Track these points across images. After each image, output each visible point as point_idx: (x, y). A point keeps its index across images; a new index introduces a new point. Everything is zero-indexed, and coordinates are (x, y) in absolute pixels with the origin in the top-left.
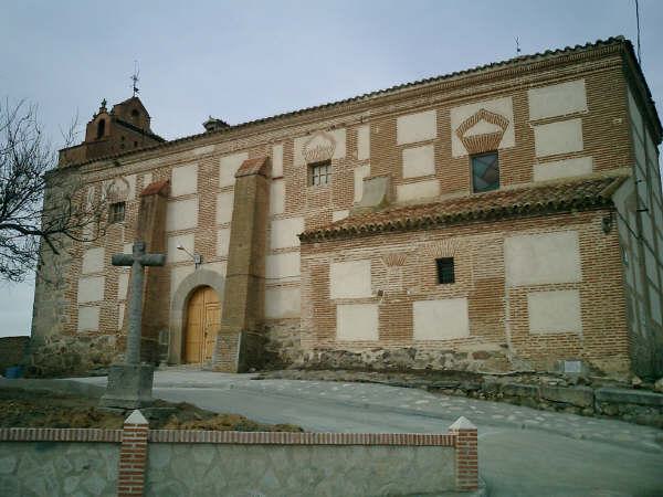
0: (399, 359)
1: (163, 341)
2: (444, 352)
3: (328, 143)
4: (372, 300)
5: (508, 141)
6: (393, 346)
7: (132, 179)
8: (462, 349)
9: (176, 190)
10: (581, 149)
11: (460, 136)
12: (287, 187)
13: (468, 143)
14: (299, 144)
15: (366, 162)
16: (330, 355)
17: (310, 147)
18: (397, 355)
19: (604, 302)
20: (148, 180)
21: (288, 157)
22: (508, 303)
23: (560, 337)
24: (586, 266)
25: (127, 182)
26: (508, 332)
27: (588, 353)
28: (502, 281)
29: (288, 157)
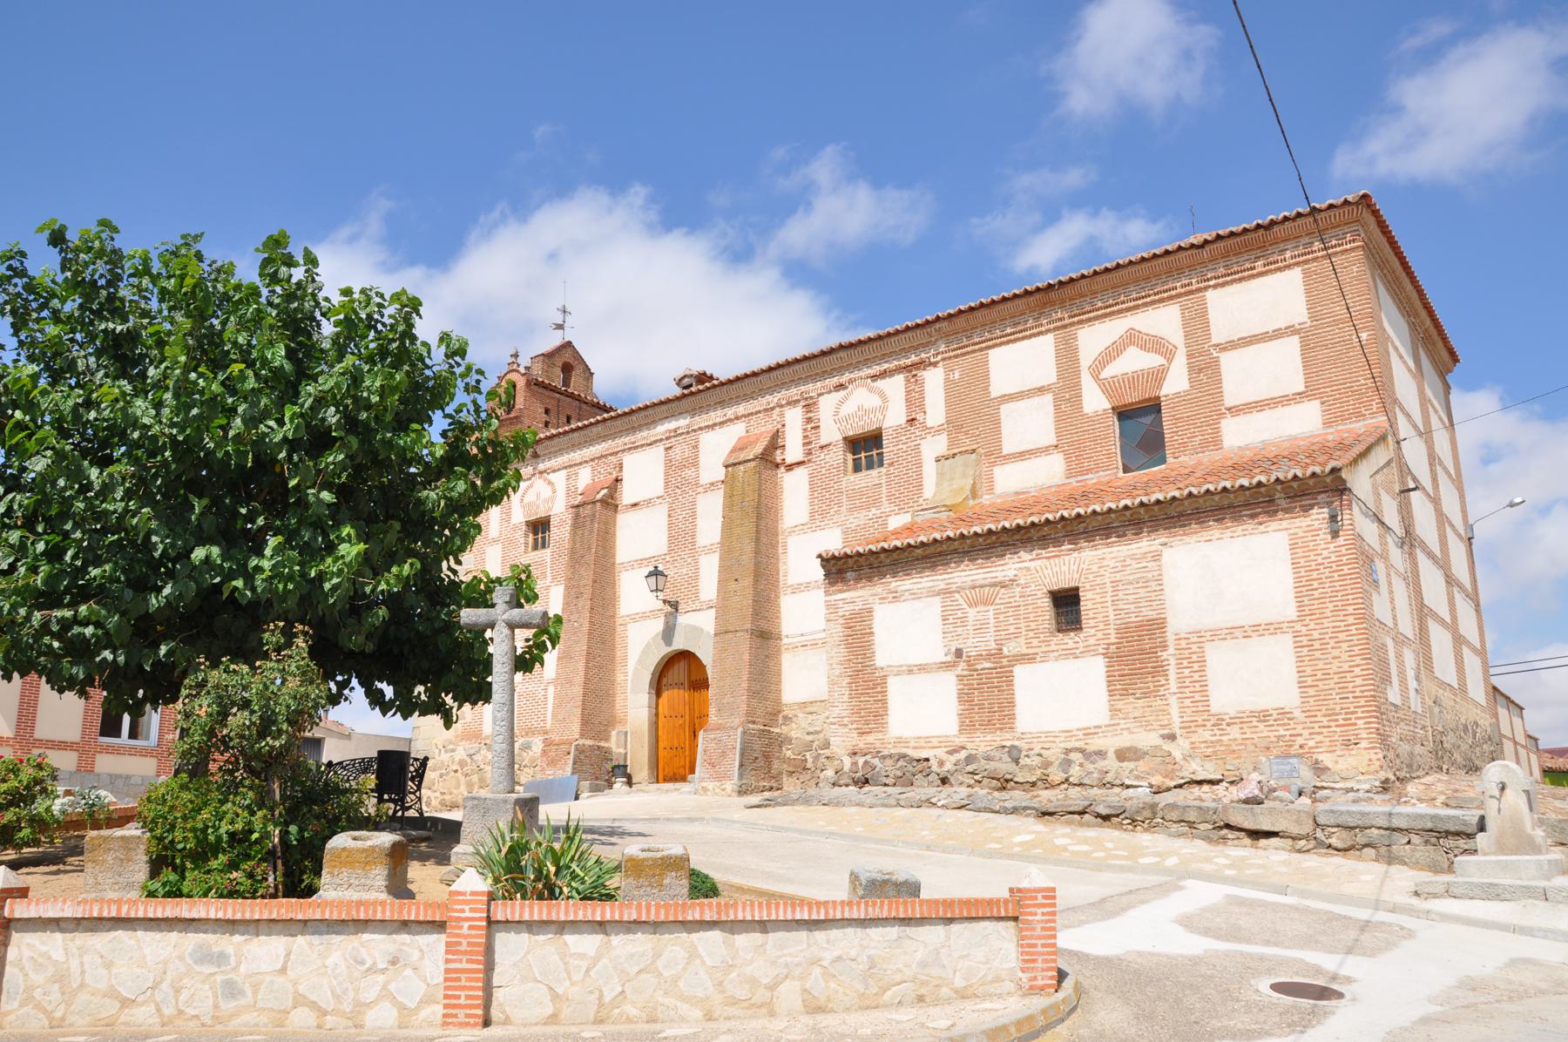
0: (992, 765)
1: (618, 747)
2: (1068, 751)
3: (873, 401)
4: (946, 666)
5: (1176, 383)
6: (982, 743)
7: (559, 478)
8: (1095, 744)
10: (1301, 388)
11: (1096, 378)
12: (811, 476)
13: (1107, 387)
14: (827, 404)
15: (938, 431)
16: (876, 761)
17: (849, 408)
18: (988, 759)
19: (1335, 653)
20: (585, 477)
21: (811, 424)
22: (1173, 662)
23: (1263, 716)
24: (1304, 590)
25: (550, 483)
26: (1175, 711)
27: (1311, 743)
28: (1156, 626)
29: (811, 424)
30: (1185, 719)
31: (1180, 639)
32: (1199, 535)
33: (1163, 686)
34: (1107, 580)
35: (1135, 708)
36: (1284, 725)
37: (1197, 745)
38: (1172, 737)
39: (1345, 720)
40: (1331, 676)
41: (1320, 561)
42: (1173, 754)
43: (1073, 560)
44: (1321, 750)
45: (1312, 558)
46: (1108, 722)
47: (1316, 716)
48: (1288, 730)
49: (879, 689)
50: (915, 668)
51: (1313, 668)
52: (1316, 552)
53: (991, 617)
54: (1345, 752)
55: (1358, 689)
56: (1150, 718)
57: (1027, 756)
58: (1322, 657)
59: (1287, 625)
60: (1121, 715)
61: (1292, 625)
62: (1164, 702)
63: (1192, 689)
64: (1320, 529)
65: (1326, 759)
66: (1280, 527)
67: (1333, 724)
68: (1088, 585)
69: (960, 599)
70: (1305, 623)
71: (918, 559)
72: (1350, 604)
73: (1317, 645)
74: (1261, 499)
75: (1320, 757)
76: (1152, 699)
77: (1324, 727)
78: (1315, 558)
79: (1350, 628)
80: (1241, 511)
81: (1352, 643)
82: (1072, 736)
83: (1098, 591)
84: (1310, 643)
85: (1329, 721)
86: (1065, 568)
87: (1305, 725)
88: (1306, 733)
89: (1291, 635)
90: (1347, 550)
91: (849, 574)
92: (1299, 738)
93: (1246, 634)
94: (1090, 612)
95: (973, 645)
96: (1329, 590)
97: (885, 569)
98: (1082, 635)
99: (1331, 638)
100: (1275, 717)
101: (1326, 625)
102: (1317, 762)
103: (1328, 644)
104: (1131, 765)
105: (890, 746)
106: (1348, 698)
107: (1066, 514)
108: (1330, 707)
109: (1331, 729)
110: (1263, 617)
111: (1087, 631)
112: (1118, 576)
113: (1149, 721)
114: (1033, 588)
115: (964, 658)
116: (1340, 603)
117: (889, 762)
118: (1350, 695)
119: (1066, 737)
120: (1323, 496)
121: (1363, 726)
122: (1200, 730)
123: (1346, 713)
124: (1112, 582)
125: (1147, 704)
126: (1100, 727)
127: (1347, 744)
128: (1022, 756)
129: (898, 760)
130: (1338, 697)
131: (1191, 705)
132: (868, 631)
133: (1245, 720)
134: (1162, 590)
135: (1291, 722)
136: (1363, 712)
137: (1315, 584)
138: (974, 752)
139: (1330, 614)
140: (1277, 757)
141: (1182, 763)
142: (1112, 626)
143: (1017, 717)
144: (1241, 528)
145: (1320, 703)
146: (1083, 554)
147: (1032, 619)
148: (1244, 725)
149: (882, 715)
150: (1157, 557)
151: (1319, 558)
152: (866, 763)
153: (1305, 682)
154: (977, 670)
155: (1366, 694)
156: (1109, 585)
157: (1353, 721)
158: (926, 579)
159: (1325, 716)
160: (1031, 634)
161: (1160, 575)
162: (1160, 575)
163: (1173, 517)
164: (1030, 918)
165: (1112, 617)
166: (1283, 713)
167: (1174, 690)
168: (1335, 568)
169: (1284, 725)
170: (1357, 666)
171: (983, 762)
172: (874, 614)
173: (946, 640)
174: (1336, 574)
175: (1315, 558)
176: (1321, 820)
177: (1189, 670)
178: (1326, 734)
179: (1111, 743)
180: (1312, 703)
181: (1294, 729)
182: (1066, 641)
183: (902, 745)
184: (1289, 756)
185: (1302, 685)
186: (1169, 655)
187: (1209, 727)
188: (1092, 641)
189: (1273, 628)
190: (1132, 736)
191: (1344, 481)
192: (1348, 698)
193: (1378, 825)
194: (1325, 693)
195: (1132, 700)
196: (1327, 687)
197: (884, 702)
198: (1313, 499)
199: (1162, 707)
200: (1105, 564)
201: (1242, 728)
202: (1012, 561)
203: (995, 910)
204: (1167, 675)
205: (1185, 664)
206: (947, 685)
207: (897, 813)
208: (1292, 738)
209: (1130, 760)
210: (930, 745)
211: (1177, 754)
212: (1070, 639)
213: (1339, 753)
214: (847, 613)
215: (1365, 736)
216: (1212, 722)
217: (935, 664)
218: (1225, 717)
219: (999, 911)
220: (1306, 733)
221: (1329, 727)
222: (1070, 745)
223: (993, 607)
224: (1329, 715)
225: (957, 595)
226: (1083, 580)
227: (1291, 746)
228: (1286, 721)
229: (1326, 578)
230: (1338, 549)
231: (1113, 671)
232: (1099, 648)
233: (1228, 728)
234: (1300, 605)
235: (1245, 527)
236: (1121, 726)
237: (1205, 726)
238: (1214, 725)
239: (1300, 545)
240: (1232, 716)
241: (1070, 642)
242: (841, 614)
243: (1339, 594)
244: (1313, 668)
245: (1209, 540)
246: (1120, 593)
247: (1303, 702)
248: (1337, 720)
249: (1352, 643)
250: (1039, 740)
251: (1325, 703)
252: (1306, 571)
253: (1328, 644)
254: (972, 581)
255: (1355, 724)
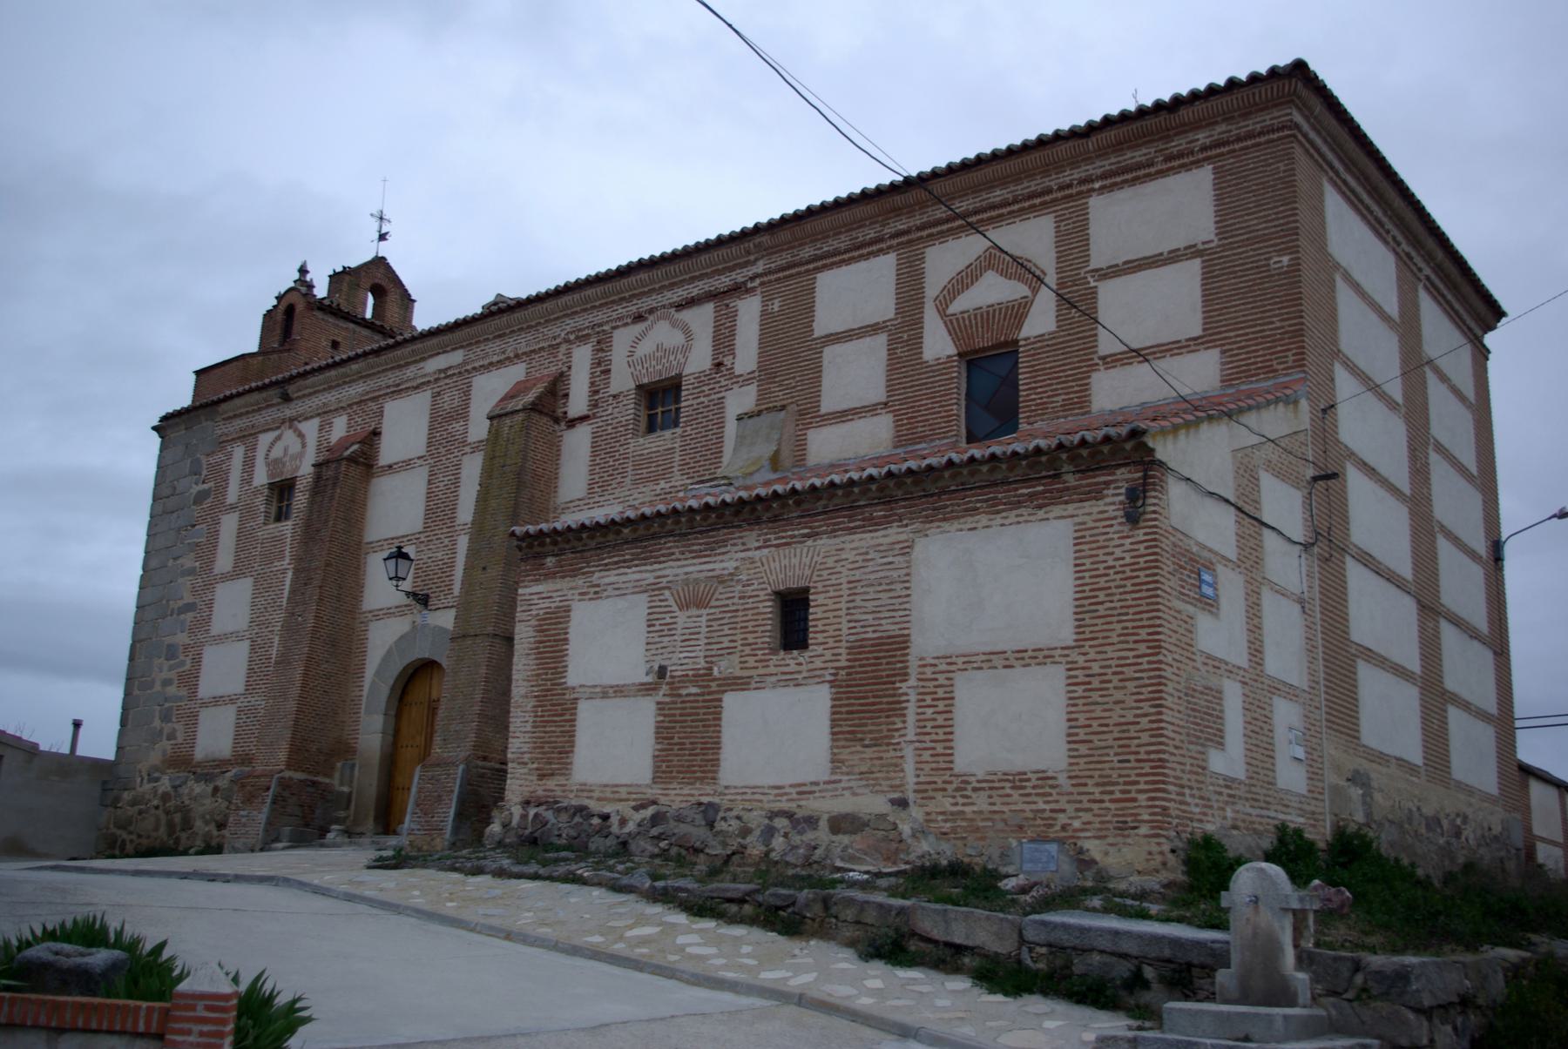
0: (682, 829)
1: (342, 784)
2: (773, 815)
3: (677, 338)
4: (646, 689)
5: (1041, 320)
6: (678, 797)
7: (310, 428)
8: (813, 805)
9: (388, 451)
10: (1197, 331)
11: (942, 313)
12: (595, 436)
13: (956, 326)
14: (622, 339)
15: (747, 380)
16: (549, 815)
17: (646, 347)
18: (679, 819)
19: (1118, 695)
20: (340, 428)
22: (913, 697)
23: (1018, 780)
24: (1086, 604)
25: (301, 435)
26: (909, 767)
27: (1077, 824)
28: (899, 644)
29: (601, 368)
30: (922, 779)
31: (925, 666)
32: (962, 520)
33: (897, 730)
34: (844, 580)
35: (862, 759)
36: (1044, 795)
37: (933, 816)
38: (902, 803)
39: (1123, 792)
40: (1111, 728)
41: (1111, 563)
42: (900, 826)
43: (805, 550)
44: (1088, 834)
45: (1102, 558)
46: (826, 778)
47: (1086, 785)
48: (1048, 802)
49: (567, 717)
50: (611, 691)
51: (1088, 715)
52: (1107, 550)
53: (704, 624)
54: (1120, 839)
55: (1142, 750)
56: (878, 775)
57: (724, 819)
58: (1100, 700)
59: (1059, 652)
60: (844, 769)
61: (1066, 652)
62: (899, 754)
63: (934, 737)
64: (1115, 518)
65: (1094, 848)
66: (1065, 514)
67: (1106, 797)
68: (819, 585)
69: (671, 599)
70: (1083, 650)
71: (627, 543)
72: (1143, 627)
73: (1096, 683)
74: (1044, 473)
75: (1087, 845)
76: (884, 748)
77: (1095, 801)
78: (1105, 558)
79: (1140, 660)
80: (1017, 489)
81: (1141, 682)
82: (781, 795)
83: (832, 594)
84: (1087, 679)
85: (1102, 793)
86: (795, 561)
87: (1072, 798)
88: (1070, 808)
89: (1062, 668)
90: (1146, 548)
91: (549, 559)
92: (1061, 816)
93: (1007, 663)
94: (819, 623)
95: (682, 661)
96: (1118, 605)
97: (588, 554)
98: (807, 654)
99: (1115, 673)
100: (1034, 782)
101: (1110, 655)
102: (1081, 851)
103: (1110, 681)
104: (845, 839)
105: (572, 796)
106: (1128, 761)
107: (798, 486)
108: (1104, 773)
109: (1104, 805)
110: (1029, 640)
111: (815, 649)
112: (858, 575)
113: (876, 779)
114: (755, 587)
115: (668, 679)
116: (1129, 624)
117: (564, 817)
118: (1132, 757)
119: (776, 795)
120: (1123, 470)
121: (1144, 803)
122: (939, 795)
123: (1126, 783)
124: (849, 582)
125: (876, 755)
126: (816, 784)
127: (1123, 828)
128: (719, 818)
129: (574, 814)
130: (1116, 759)
131: (930, 759)
132: (562, 637)
133: (996, 785)
134: (908, 595)
135: (1054, 792)
136: (1146, 783)
137: (1102, 596)
138: (664, 809)
139: (1115, 640)
140: (1032, 840)
141: (909, 841)
142: (844, 644)
143: (722, 764)
144: (1015, 512)
145: (1092, 766)
146: (819, 542)
147: (750, 629)
148: (994, 793)
149: (567, 752)
150: (906, 549)
151: (1109, 558)
152: (536, 815)
153: (1077, 734)
154: (680, 695)
155: (1152, 756)
156: (845, 586)
157: (1133, 795)
158: (634, 569)
159: (1097, 785)
160: (747, 650)
161: (908, 575)
162: (908, 575)
163: (932, 495)
164: (179, 1038)
165: (845, 631)
166: (1044, 778)
167: (911, 736)
168: (1129, 574)
169: (1044, 795)
170: (1146, 715)
171: (672, 823)
172: (572, 614)
173: (648, 654)
174: (1128, 583)
175: (1105, 558)
176: (1030, 935)
177: (932, 710)
178: (1096, 812)
179: (825, 806)
180: (1082, 766)
181: (1057, 801)
182: (788, 662)
183: (585, 794)
184: (1046, 840)
185: (1072, 740)
186: (909, 688)
187: (950, 792)
188: (818, 663)
189: (1037, 657)
190: (855, 798)
191: (1151, 451)
192: (1128, 761)
193: (1102, 948)
194: (1099, 752)
195: (859, 748)
196: (1103, 744)
197: (570, 735)
198: (1109, 475)
199: (894, 761)
200: (844, 557)
201: (990, 797)
202: (736, 548)
203: (130, 1020)
204: (904, 715)
205: (929, 702)
206: (644, 714)
207: (523, 886)
208: (1054, 815)
209: (845, 833)
210: (617, 796)
211: (906, 829)
212: (792, 660)
213: (1111, 840)
214: (541, 612)
215: (1146, 817)
216: (955, 786)
217: (634, 684)
218: (973, 779)
219: (136, 1022)
220: (1070, 808)
221: (1102, 801)
222: (777, 806)
223: (708, 611)
224: (1104, 784)
225: (667, 593)
226: (815, 578)
227: (1051, 826)
228: (1048, 790)
229: (1117, 587)
230: (1136, 547)
231: (840, 706)
232: (826, 672)
233: (974, 795)
234: (1080, 626)
235: (1019, 512)
236: (843, 785)
237: (945, 790)
238: (957, 790)
239: (1088, 539)
240: (980, 778)
241: (792, 662)
242: (534, 613)
243: (1131, 610)
244: (1088, 715)
245: (975, 528)
246: (858, 598)
247: (1071, 764)
248: (1112, 792)
249: (1141, 682)
250: (745, 797)
251: (1099, 766)
252: (1091, 577)
253: (1110, 681)
254: (686, 573)
255: (1134, 800)
